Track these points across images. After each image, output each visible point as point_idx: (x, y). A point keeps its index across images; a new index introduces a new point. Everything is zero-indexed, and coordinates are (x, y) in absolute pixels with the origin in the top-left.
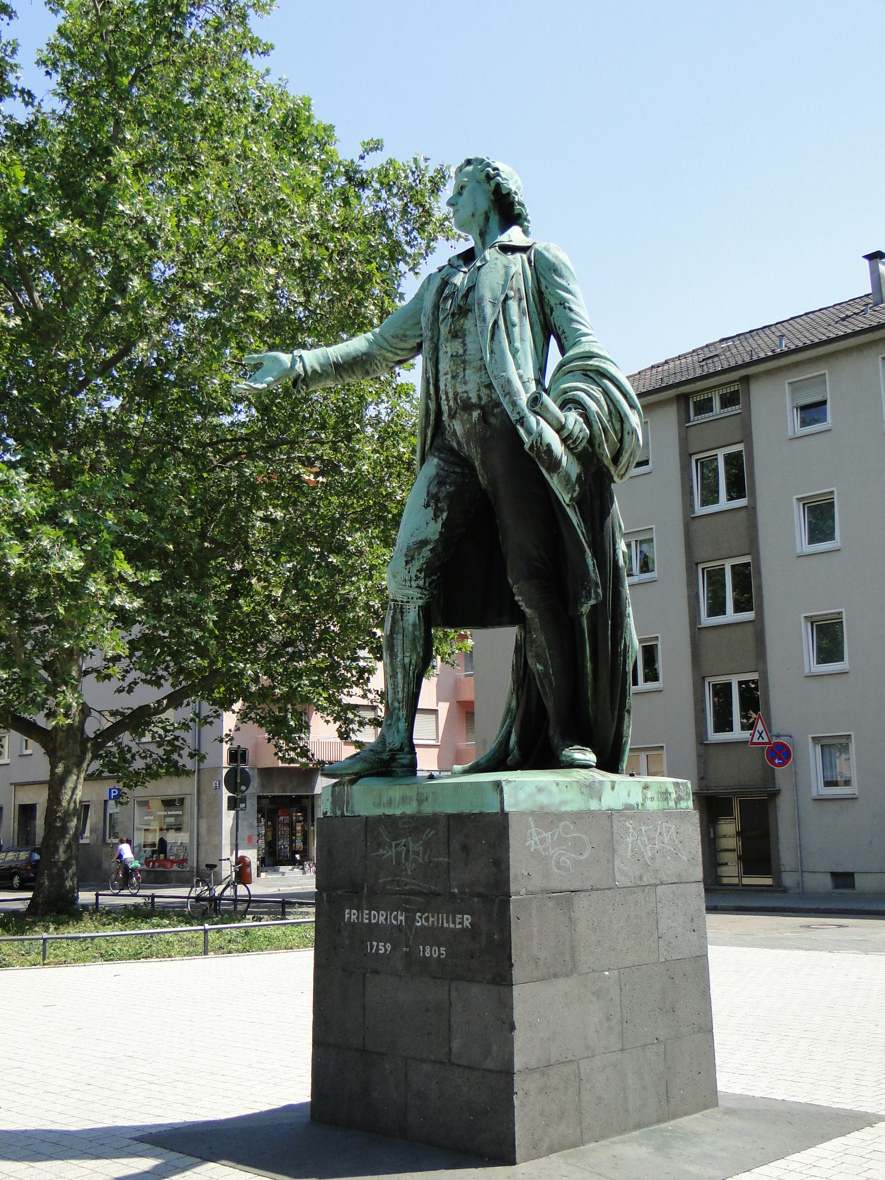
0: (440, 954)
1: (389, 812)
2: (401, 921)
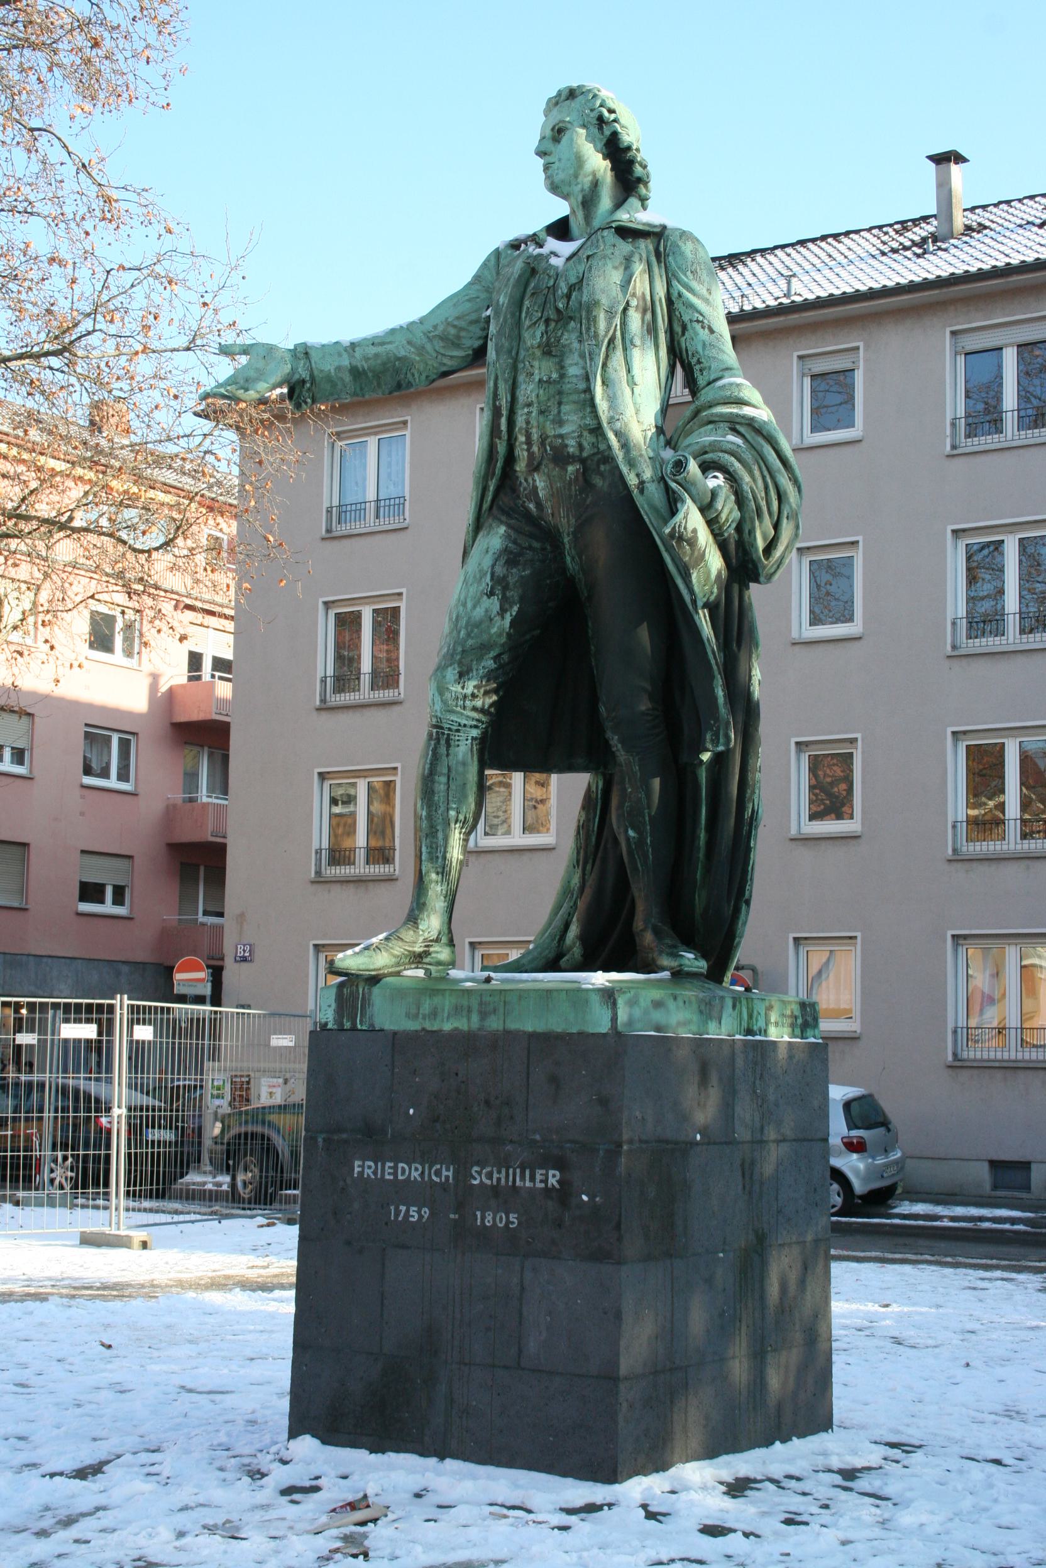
0: (508, 1222)
1: (430, 1026)
2: (447, 1177)
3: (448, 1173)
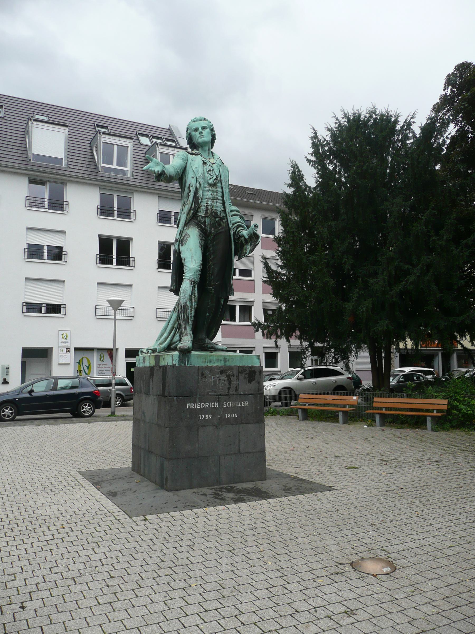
0: (235, 416)
2: (216, 406)
3: (217, 405)
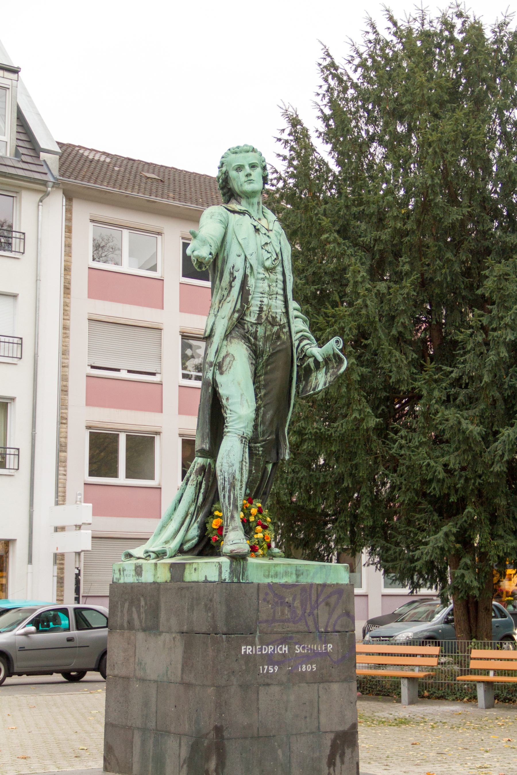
0: (312, 669)
2: (285, 651)
